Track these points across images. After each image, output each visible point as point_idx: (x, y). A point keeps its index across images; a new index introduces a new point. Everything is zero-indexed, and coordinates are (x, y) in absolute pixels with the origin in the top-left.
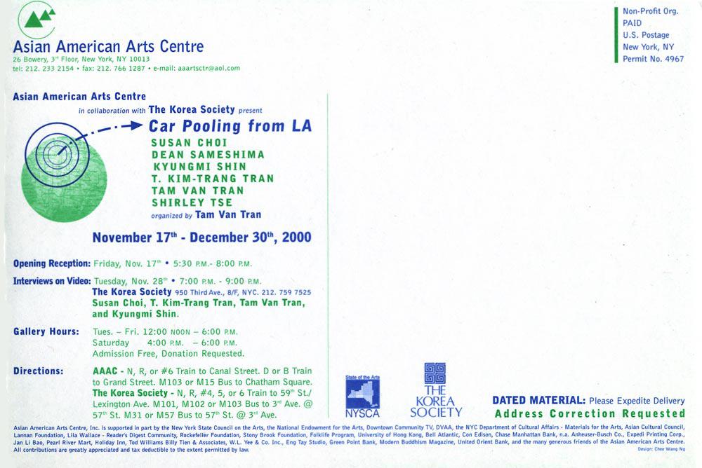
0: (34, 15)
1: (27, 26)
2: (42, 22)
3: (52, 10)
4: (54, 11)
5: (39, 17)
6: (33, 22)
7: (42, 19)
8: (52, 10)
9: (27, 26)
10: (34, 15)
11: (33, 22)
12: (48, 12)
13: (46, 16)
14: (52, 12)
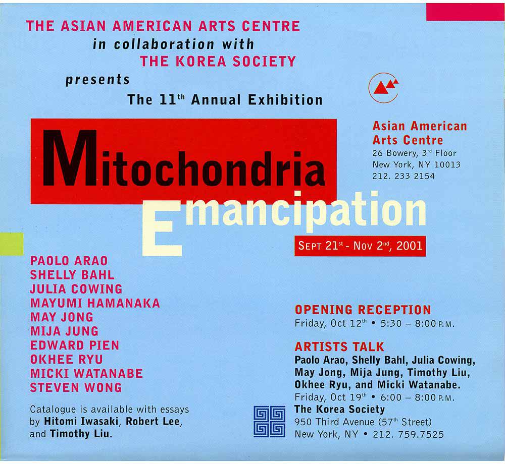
0: (381, 84)
1: (375, 93)
2: (387, 89)
3: (396, 80)
4: (398, 81)
5: (385, 85)
6: (381, 90)
7: (387, 87)
8: (396, 80)
9: (375, 93)
10: (381, 84)
11: (381, 90)
12: (393, 82)
13: (391, 85)
14: (396, 82)
